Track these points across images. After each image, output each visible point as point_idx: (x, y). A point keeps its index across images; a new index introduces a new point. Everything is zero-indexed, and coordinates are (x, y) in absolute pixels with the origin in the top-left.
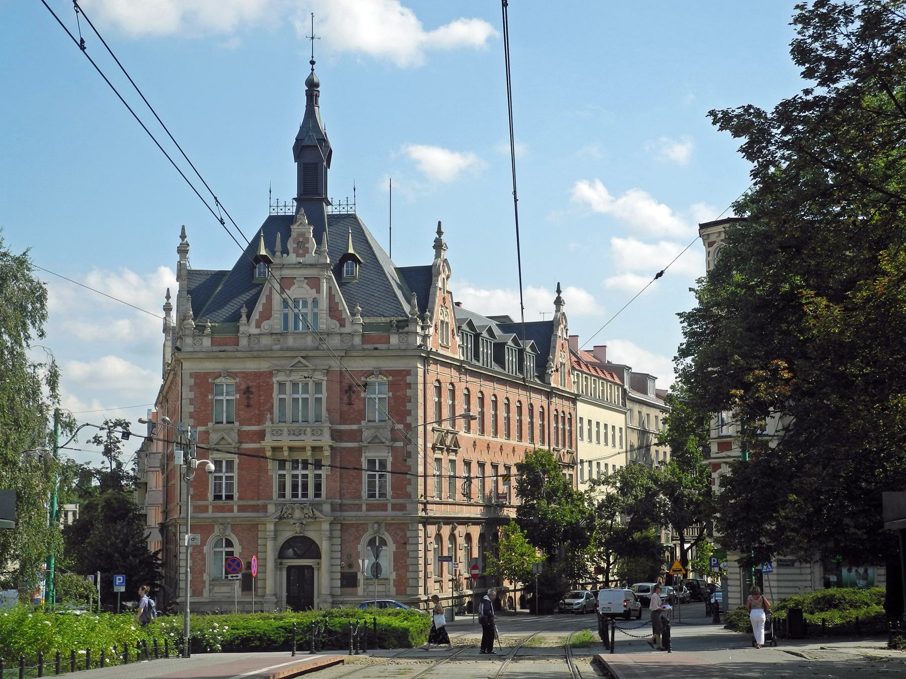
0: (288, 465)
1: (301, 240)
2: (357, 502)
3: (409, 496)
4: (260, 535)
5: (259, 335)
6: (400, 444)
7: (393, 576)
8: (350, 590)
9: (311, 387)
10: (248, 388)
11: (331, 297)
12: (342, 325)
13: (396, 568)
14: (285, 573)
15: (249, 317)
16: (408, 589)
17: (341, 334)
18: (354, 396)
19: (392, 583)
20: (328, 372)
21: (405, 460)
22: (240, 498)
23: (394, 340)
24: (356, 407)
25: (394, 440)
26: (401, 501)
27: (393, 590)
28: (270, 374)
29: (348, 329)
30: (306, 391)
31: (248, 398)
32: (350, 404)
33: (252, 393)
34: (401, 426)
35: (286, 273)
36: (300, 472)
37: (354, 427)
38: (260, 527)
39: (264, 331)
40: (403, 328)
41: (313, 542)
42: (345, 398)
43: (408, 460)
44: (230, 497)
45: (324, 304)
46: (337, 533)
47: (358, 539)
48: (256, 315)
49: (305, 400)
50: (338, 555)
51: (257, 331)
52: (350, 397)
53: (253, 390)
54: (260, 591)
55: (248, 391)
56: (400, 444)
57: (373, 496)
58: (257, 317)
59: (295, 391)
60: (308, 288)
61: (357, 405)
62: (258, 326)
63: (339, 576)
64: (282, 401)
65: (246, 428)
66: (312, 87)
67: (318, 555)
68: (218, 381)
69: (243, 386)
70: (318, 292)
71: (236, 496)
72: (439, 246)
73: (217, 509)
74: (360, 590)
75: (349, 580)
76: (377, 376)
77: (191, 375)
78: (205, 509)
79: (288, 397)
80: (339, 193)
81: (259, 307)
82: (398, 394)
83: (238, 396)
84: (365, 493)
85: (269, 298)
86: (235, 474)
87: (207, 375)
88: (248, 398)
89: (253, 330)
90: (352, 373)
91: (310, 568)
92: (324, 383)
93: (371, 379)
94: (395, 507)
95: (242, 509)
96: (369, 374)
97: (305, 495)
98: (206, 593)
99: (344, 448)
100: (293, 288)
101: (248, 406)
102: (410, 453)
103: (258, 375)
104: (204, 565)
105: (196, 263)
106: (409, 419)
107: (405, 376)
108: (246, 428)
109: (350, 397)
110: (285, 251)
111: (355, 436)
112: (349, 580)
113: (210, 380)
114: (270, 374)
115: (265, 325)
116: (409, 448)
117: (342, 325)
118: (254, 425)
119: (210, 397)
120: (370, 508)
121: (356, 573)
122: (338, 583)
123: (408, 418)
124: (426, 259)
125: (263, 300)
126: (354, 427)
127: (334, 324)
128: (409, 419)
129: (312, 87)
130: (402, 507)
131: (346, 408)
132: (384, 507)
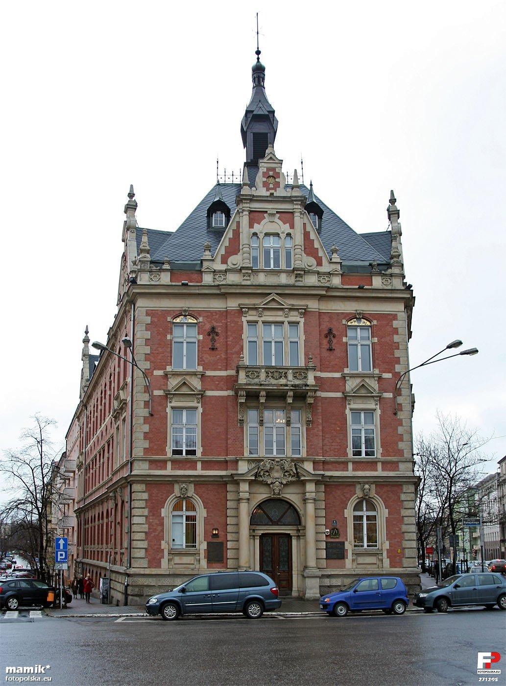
1: (271, 173)
2: (342, 459)
3: (401, 453)
4: (230, 496)
5: (226, 271)
6: (390, 395)
7: (387, 545)
8: (337, 562)
10: (213, 328)
11: (306, 235)
12: (320, 264)
13: (390, 537)
14: (257, 542)
16: (404, 560)
17: (318, 273)
18: (335, 341)
19: (385, 554)
20: (305, 312)
21: (395, 414)
22: (203, 454)
23: (377, 282)
25: (383, 390)
26: (394, 459)
27: (387, 562)
28: (240, 312)
29: (326, 268)
31: (213, 340)
32: (330, 350)
33: (217, 334)
37: (337, 375)
38: (230, 487)
39: (230, 266)
40: (385, 270)
41: (291, 506)
42: (325, 341)
43: (399, 413)
44: (193, 452)
45: (299, 239)
50: (323, 521)
51: (223, 267)
52: (330, 342)
53: (218, 330)
54: (230, 563)
55: (213, 331)
56: (390, 395)
57: (359, 453)
58: (223, 252)
60: (280, 223)
61: (338, 352)
62: (224, 261)
63: (323, 545)
65: (209, 373)
67: (297, 520)
68: (178, 320)
69: (208, 327)
70: (292, 226)
73: (176, 464)
74: (348, 562)
75: (335, 552)
76: (359, 319)
77: (147, 314)
78: (162, 464)
82: (383, 340)
83: (201, 337)
84: (350, 451)
85: (237, 233)
87: (166, 313)
88: (213, 340)
89: (219, 266)
90: (331, 315)
91: (289, 536)
92: (302, 325)
93: (354, 323)
94: (386, 465)
95: (207, 465)
98: (164, 563)
99: (326, 398)
100: (263, 222)
101: (213, 349)
102: (400, 405)
103: (226, 313)
104: (162, 531)
105: (145, 220)
106: (398, 368)
107: (392, 320)
108: (209, 373)
109: (330, 342)
111: (338, 384)
112: (335, 552)
113: (169, 319)
115: (236, 260)
116: (400, 400)
117: (320, 264)
118: (220, 370)
119: (169, 337)
120: (358, 465)
121: (344, 543)
122: (323, 554)
123: (397, 366)
126: (337, 375)
127: (312, 261)
128: (398, 368)
130: (394, 465)
131: (326, 354)
132: (372, 465)
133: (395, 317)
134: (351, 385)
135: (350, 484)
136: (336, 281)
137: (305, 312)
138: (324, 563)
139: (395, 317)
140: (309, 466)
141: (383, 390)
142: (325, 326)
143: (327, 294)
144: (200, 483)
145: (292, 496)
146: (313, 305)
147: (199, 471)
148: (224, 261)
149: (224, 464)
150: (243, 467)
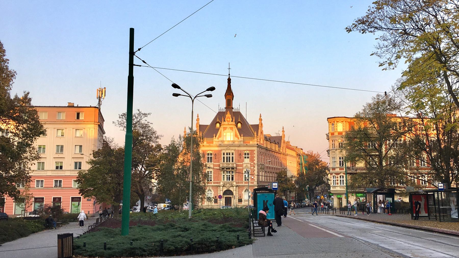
0: (225, 172)
9: (231, 154)
12: (238, 139)
15: (216, 136)
20: (235, 150)
23: (251, 143)
24: (242, 159)
28: (221, 150)
29: (240, 140)
30: (229, 155)
34: (252, 163)
35: (225, 126)
36: (228, 174)
46: (237, 189)
47: (242, 191)
48: (217, 136)
49: (229, 157)
54: (219, 203)
59: (227, 155)
64: (224, 157)
66: (229, 80)
71: (213, 180)
72: (261, 120)
79: (225, 156)
80: (235, 105)
81: (218, 134)
85: (221, 132)
86: (212, 175)
89: (217, 140)
90: (241, 151)
95: (214, 183)
96: (245, 151)
97: (229, 180)
110: (224, 121)
111: (242, 166)
112: (240, 201)
114: (221, 150)
117: (238, 139)
120: (245, 183)
124: (257, 122)
125: (219, 133)
127: (237, 138)
129: (229, 80)
130: (253, 183)
133: (254, 150)
134: (244, 165)
135: (244, 186)
136: (242, 143)
137: (235, 150)
138: (237, 203)
139: (254, 150)
140: (235, 183)
141: (251, 167)
142: (239, 153)
143: (239, 146)
144: (213, 186)
145: (231, 189)
146: (237, 148)
147: (213, 184)
148: (218, 139)
149: (218, 183)
150: (221, 183)
